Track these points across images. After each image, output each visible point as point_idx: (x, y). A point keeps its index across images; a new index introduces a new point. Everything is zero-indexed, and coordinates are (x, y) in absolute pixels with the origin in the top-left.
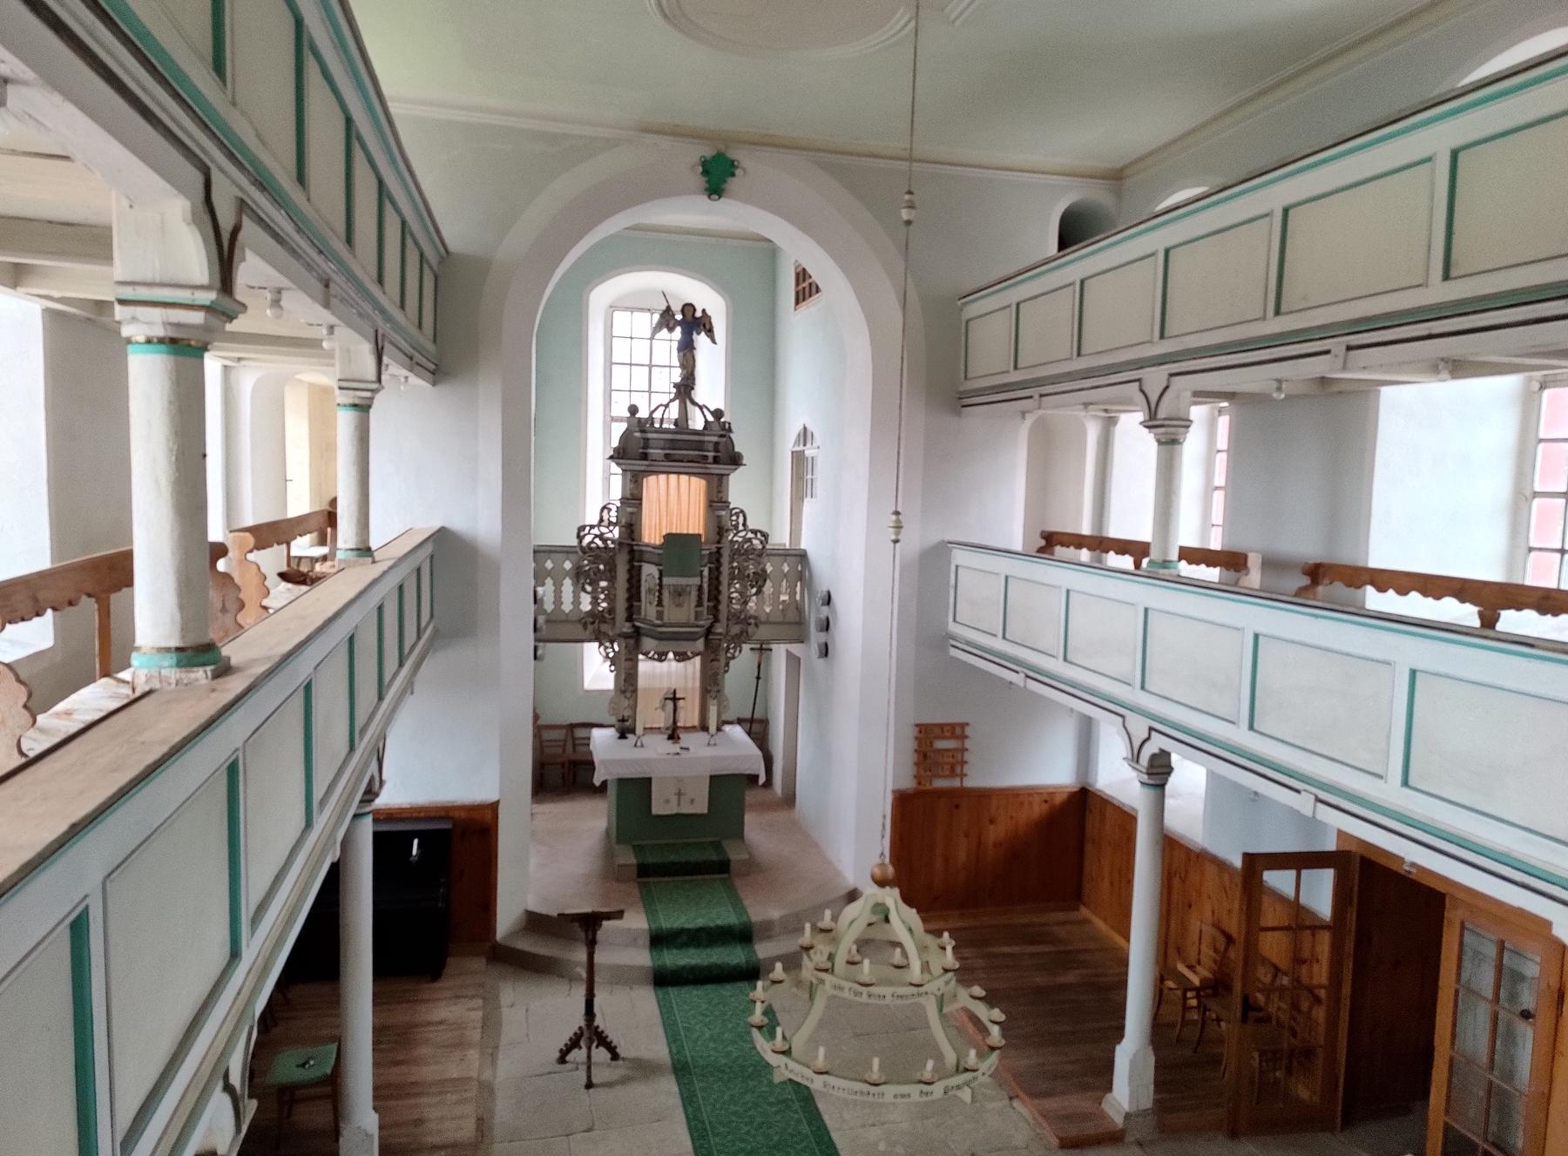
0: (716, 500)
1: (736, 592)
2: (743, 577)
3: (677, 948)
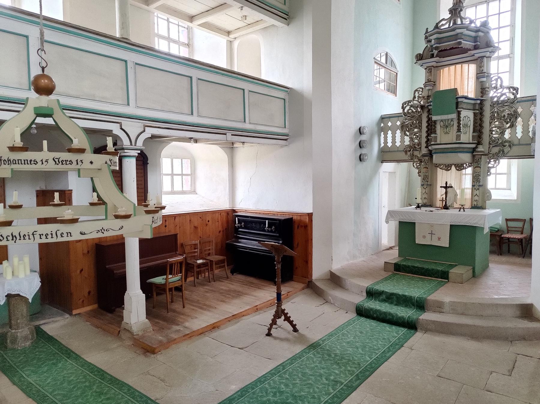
0: (481, 74)
1: (496, 127)
2: (501, 118)
3: (379, 301)
